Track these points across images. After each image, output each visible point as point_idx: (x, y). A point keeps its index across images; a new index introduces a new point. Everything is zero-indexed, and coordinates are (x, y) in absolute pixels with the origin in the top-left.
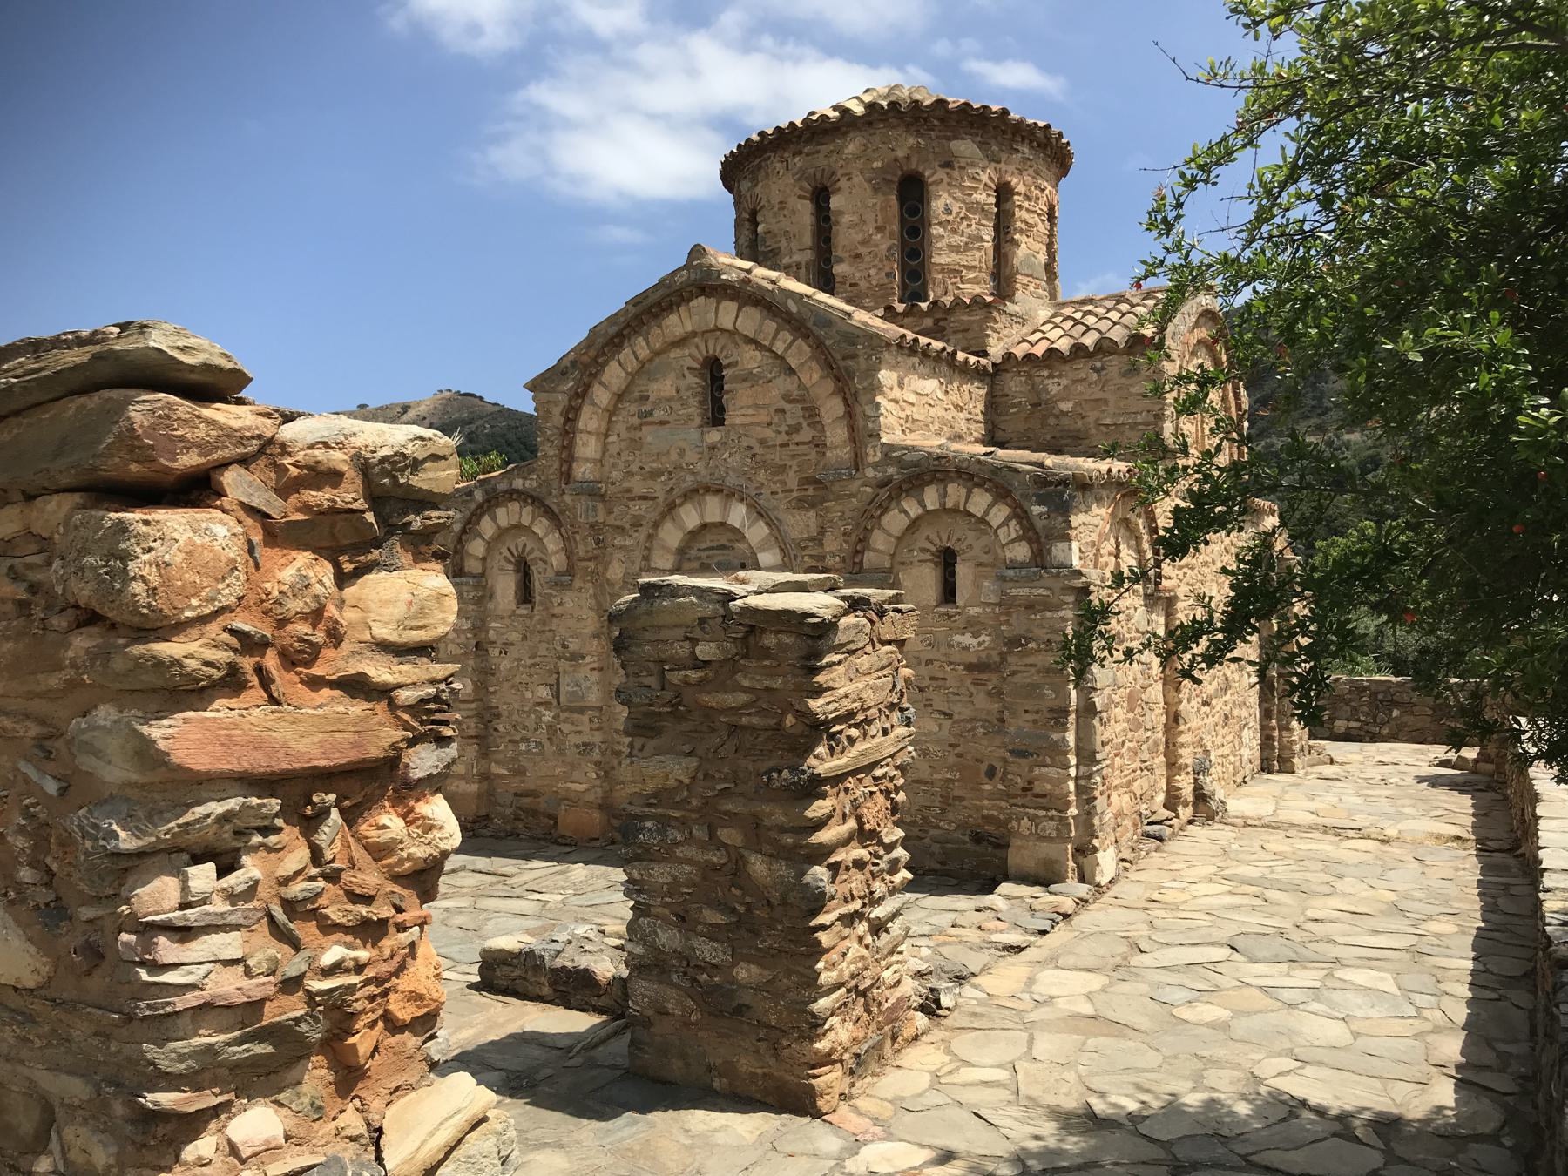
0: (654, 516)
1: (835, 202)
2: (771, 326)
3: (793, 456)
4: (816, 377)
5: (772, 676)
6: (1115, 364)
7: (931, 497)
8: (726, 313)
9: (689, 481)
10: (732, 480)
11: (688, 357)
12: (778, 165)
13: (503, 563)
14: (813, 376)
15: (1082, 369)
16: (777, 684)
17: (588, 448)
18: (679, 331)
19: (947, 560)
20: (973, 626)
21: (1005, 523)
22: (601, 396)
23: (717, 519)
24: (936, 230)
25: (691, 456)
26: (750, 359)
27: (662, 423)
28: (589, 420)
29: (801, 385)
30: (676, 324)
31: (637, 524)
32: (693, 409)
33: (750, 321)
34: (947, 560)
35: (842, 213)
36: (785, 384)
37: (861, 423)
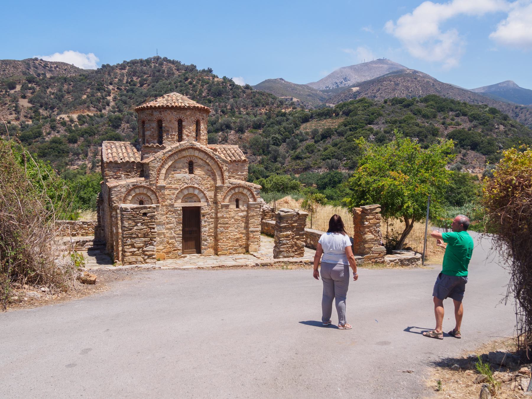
0: (177, 191)
1: (184, 123)
2: (206, 157)
3: (209, 181)
4: (215, 167)
5: (301, 221)
6: (240, 163)
7: (237, 190)
8: (197, 153)
9: (186, 186)
10: (196, 186)
11: (186, 160)
12: (169, 112)
13: (135, 201)
14: (214, 167)
15: (235, 164)
16: (302, 222)
17: (162, 176)
18: (185, 155)
19: (237, 201)
20: (243, 211)
21: (249, 195)
22: (167, 166)
23: (192, 192)
24: (201, 132)
25: (187, 181)
26: (200, 162)
27: (179, 173)
28: (164, 171)
29: (211, 168)
30: (184, 153)
31: (174, 194)
32: (187, 170)
33: (201, 155)
34: (237, 201)
35: (185, 126)
36: (207, 167)
37: (224, 176)
